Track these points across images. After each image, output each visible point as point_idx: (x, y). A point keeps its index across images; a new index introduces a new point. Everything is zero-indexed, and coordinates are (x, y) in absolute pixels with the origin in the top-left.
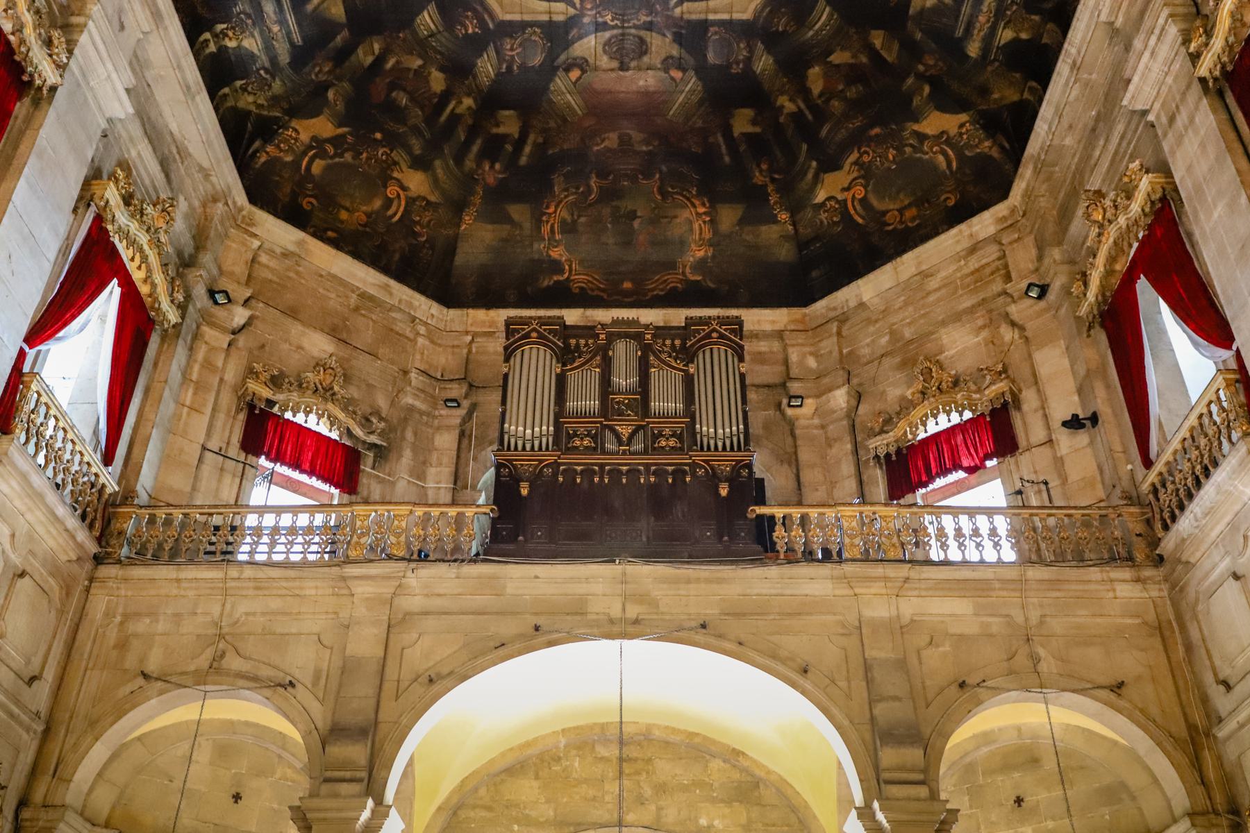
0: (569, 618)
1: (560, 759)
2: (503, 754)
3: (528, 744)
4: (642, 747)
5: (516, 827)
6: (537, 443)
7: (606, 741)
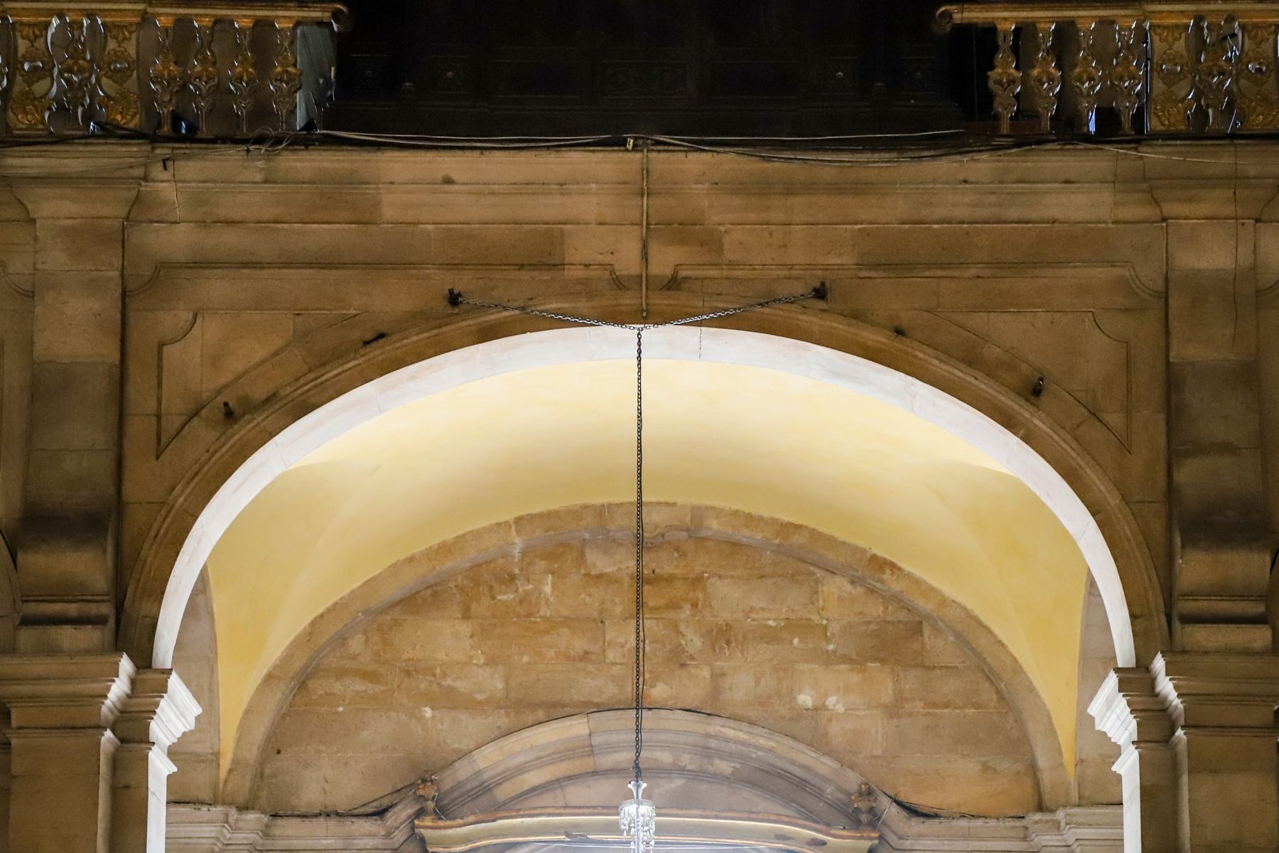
0: (525, 275)
1: (512, 578)
2: (395, 569)
4: (683, 555)
5: (428, 712)
7: (608, 543)
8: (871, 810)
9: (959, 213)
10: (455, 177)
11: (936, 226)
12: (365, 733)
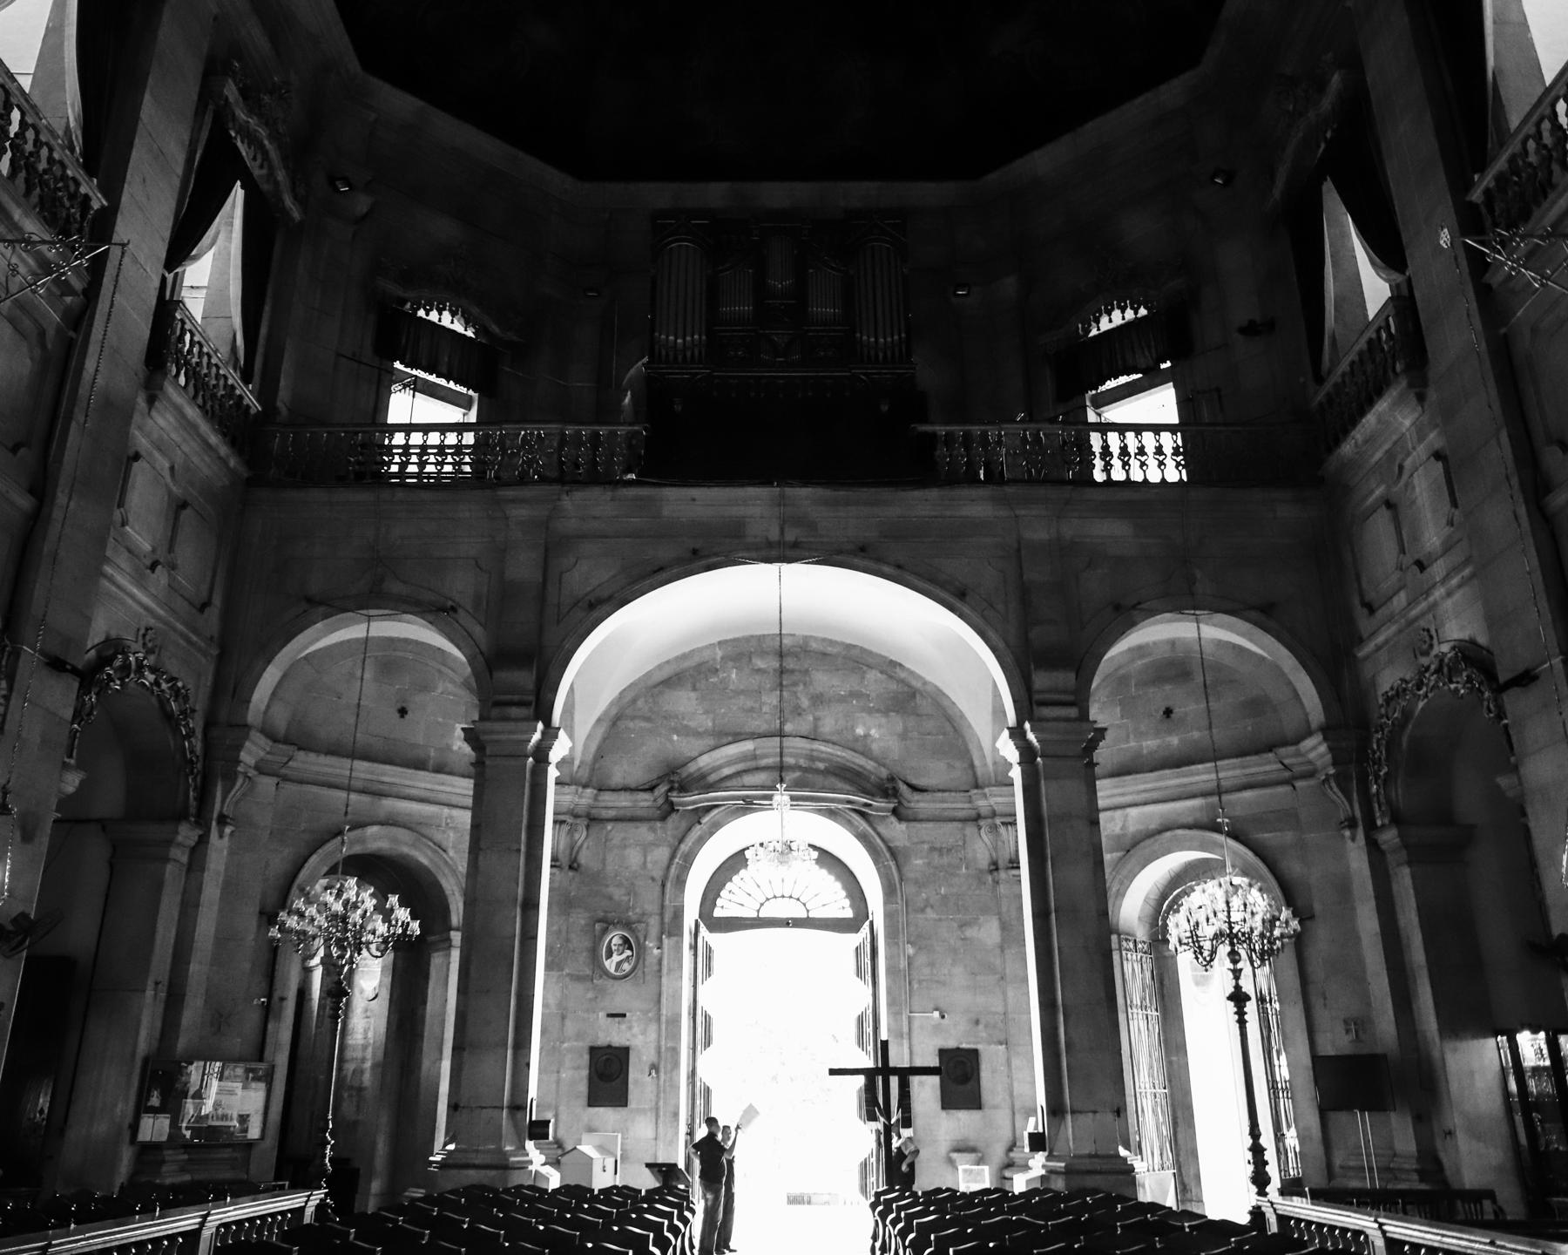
1: (717, 670)
2: (660, 667)
3: (684, 657)
4: (799, 659)
5: (675, 737)
6: (689, 354)
7: (763, 653)
8: (894, 788)
12: (644, 748)
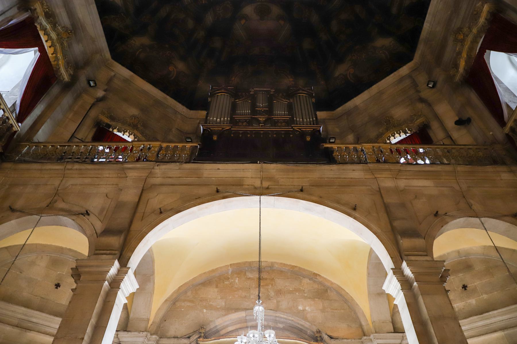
0: (234, 187)
5: (205, 311)
8: (320, 336)
9: (331, 176)
10: (220, 168)
11: (326, 179)
12: (188, 316)
